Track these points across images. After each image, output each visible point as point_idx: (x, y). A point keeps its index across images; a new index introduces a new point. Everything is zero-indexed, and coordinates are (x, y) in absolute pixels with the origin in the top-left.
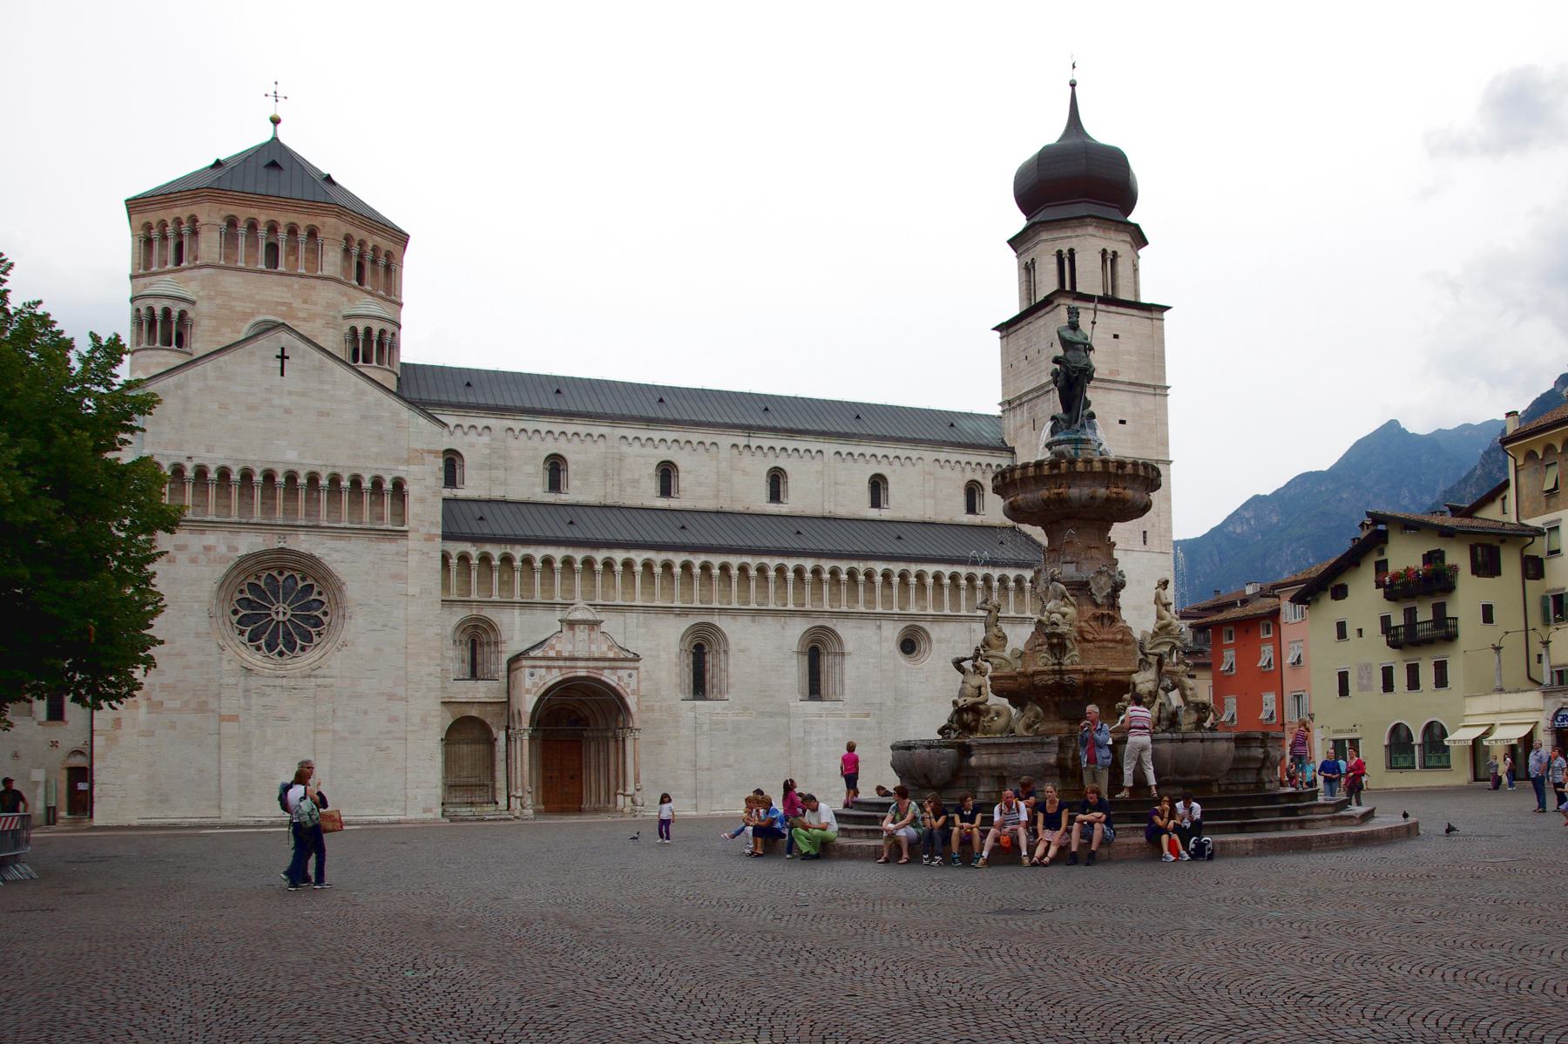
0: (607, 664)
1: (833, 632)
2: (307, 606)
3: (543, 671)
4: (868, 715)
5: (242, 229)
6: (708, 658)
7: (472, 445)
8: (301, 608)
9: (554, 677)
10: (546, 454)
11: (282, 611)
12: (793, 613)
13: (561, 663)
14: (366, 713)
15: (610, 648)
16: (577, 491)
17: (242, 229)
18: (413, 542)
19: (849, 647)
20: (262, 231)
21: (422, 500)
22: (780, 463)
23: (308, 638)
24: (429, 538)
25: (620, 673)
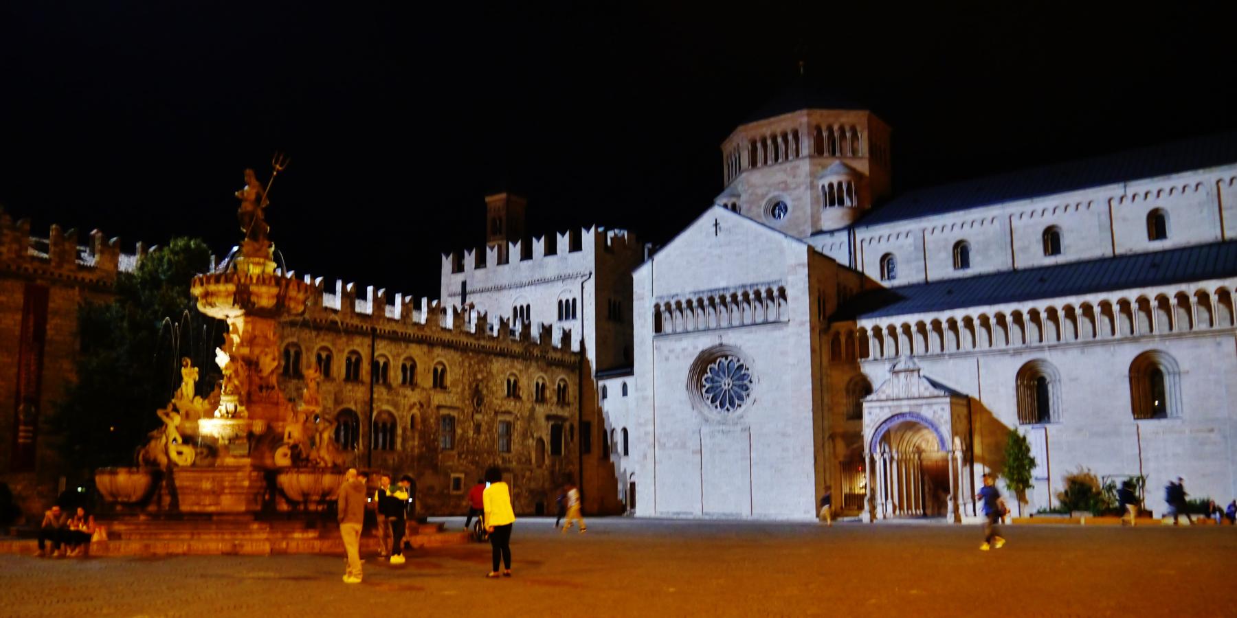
0: (924, 401)
1: (1167, 354)
2: (743, 377)
3: (878, 410)
4: (1212, 430)
5: (759, 145)
6: (1050, 388)
7: (901, 247)
8: (738, 379)
9: (886, 414)
10: (953, 242)
11: (726, 383)
12: (1122, 341)
13: (890, 403)
14: (769, 445)
15: (926, 389)
16: (979, 265)
17: (759, 145)
18: (790, 329)
19: (1184, 366)
20: (769, 142)
21: (796, 299)
22: (1160, 203)
23: (741, 398)
24: (802, 324)
25: (935, 407)
